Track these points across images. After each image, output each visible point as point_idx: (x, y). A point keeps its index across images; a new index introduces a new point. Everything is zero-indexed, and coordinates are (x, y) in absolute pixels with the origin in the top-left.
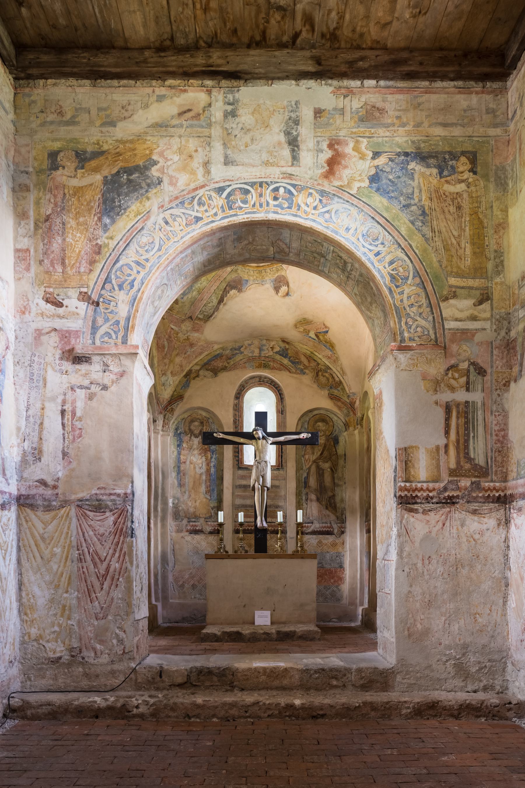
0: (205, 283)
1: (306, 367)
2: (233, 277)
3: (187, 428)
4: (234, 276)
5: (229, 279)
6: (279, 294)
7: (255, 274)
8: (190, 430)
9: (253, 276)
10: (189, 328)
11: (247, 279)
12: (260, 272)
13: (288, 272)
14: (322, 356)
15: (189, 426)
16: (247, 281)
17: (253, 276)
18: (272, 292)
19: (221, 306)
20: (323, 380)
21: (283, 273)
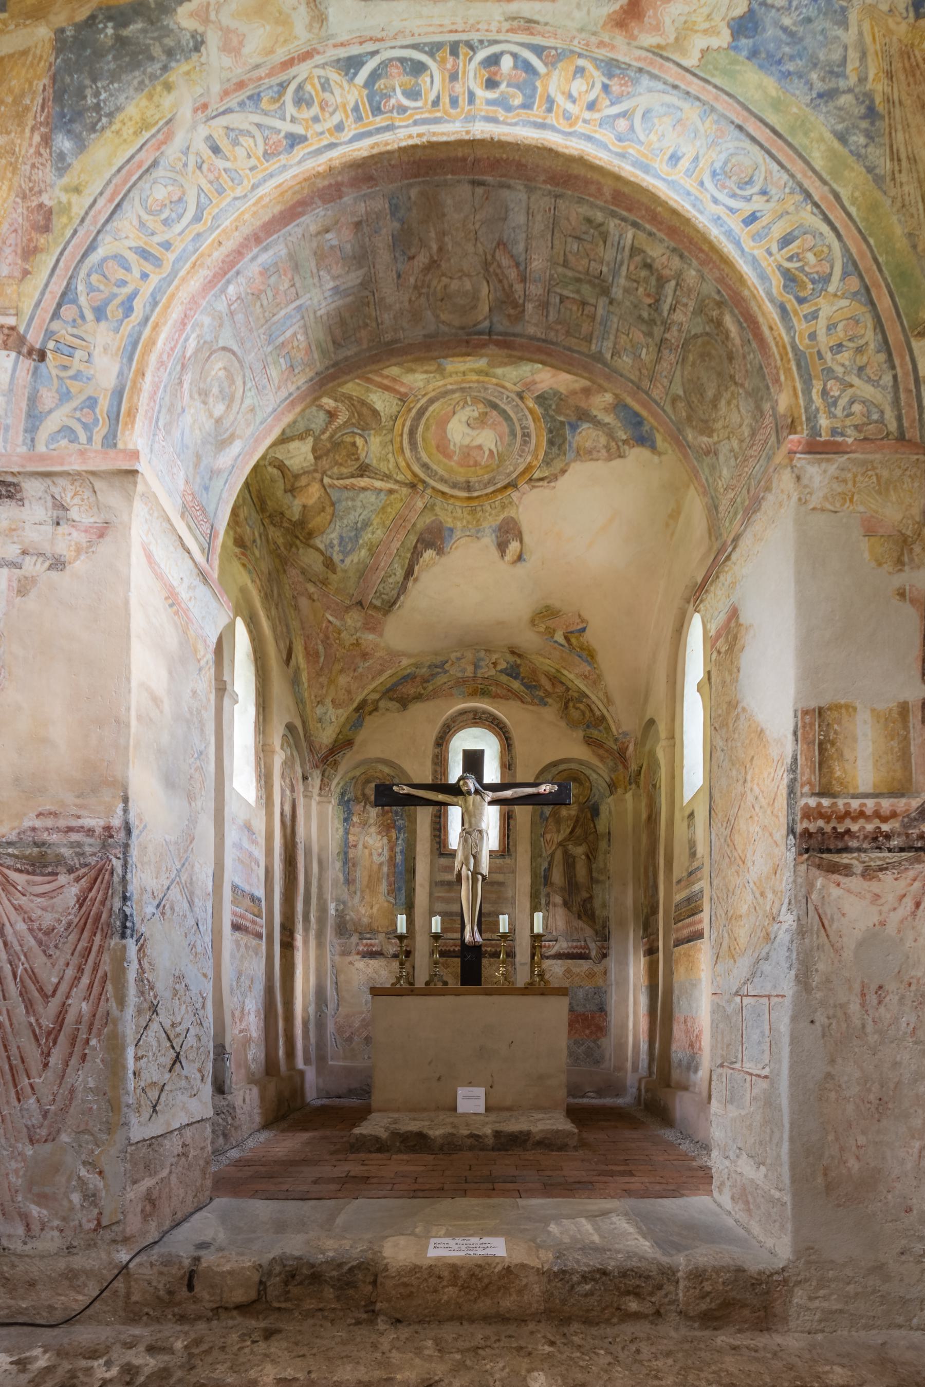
0: (379, 532)
1: (548, 694)
2: (428, 521)
3: (359, 793)
4: (428, 519)
5: (420, 526)
6: (507, 558)
7: (465, 514)
8: (364, 795)
9: (461, 519)
10: (359, 624)
11: (450, 525)
12: (473, 511)
13: (521, 509)
14: (574, 677)
15: (363, 789)
16: (451, 530)
17: (461, 519)
18: (494, 553)
19: (410, 584)
20: (575, 714)
21: (513, 513)
